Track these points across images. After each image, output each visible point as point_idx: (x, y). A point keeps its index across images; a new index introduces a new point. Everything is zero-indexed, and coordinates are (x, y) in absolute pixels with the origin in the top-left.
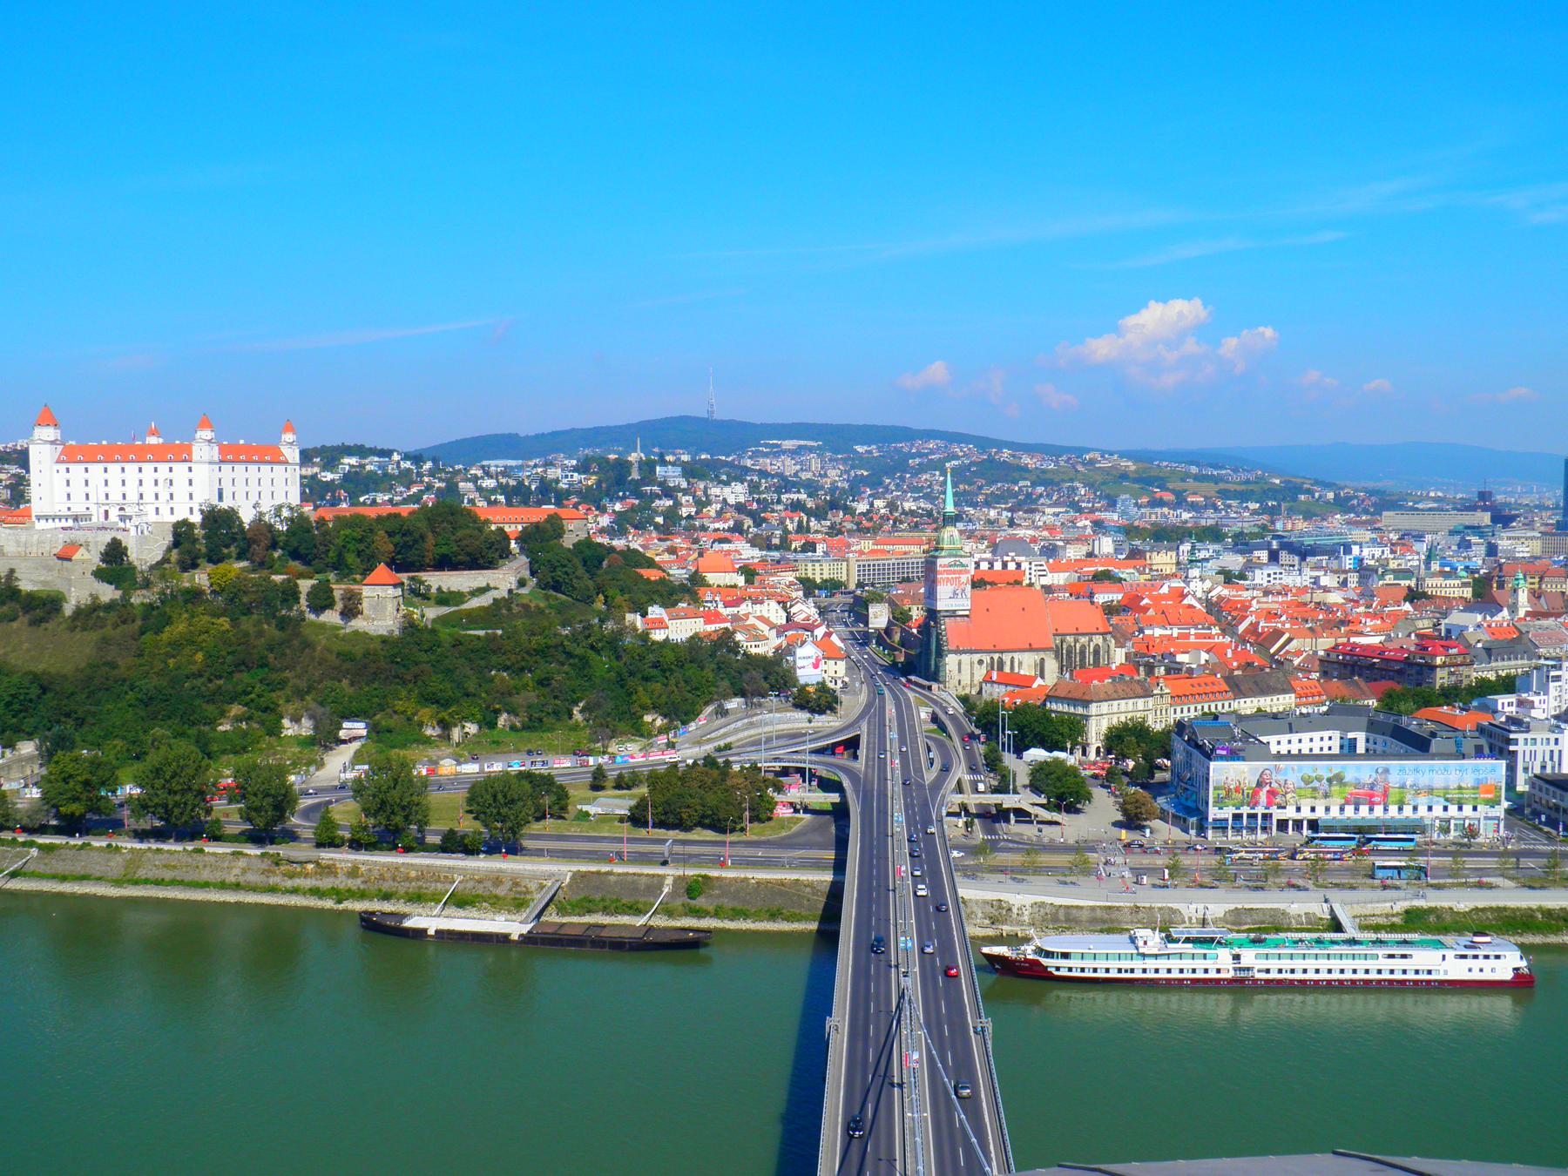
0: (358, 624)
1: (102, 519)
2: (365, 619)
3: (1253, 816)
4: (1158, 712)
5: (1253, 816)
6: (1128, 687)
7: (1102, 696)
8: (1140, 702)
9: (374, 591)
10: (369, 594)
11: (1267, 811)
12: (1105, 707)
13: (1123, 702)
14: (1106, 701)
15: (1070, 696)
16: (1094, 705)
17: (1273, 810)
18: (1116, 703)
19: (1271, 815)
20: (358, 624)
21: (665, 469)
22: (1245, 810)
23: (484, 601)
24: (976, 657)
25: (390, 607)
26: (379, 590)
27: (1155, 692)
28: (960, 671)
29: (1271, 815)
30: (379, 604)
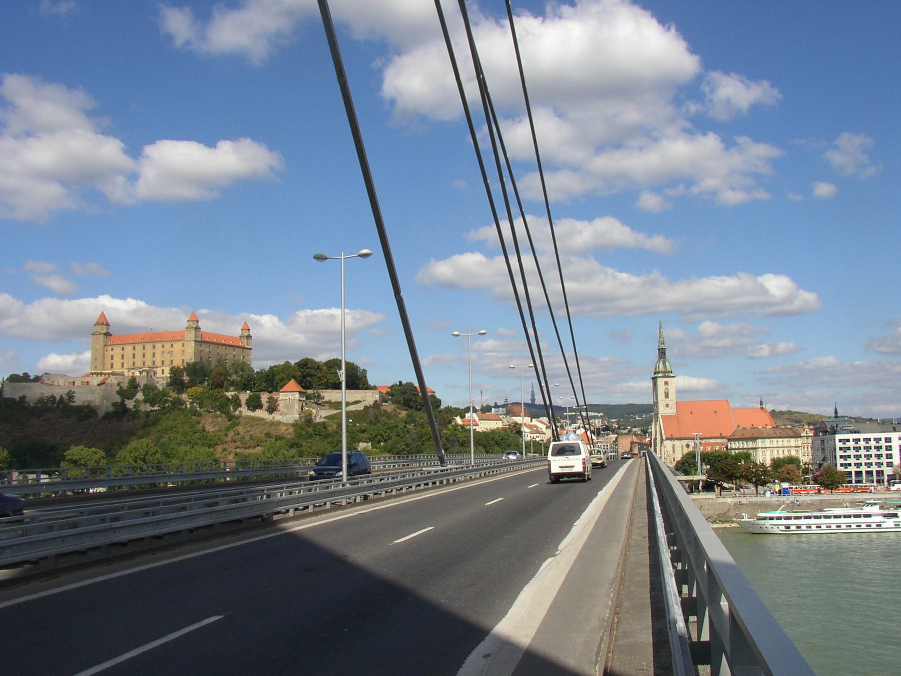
0: (277, 417)
1: (132, 365)
2: (281, 414)
3: (869, 473)
4: (806, 449)
5: (869, 473)
6: (783, 431)
7: (766, 435)
8: (792, 442)
9: (287, 396)
10: (284, 398)
11: (879, 469)
12: (767, 442)
13: (780, 440)
14: (768, 438)
15: (743, 437)
16: (760, 440)
17: (884, 468)
18: (775, 440)
19: (882, 471)
20: (277, 417)
21: (498, 409)
22: (864, 469)
23: (360, 407)
24: (685, 442)
25: (297, 406)
26: (290, 396)
27: (802, 435)
28: (674, 452)
29: (882, 471)
30: (289, 407)
